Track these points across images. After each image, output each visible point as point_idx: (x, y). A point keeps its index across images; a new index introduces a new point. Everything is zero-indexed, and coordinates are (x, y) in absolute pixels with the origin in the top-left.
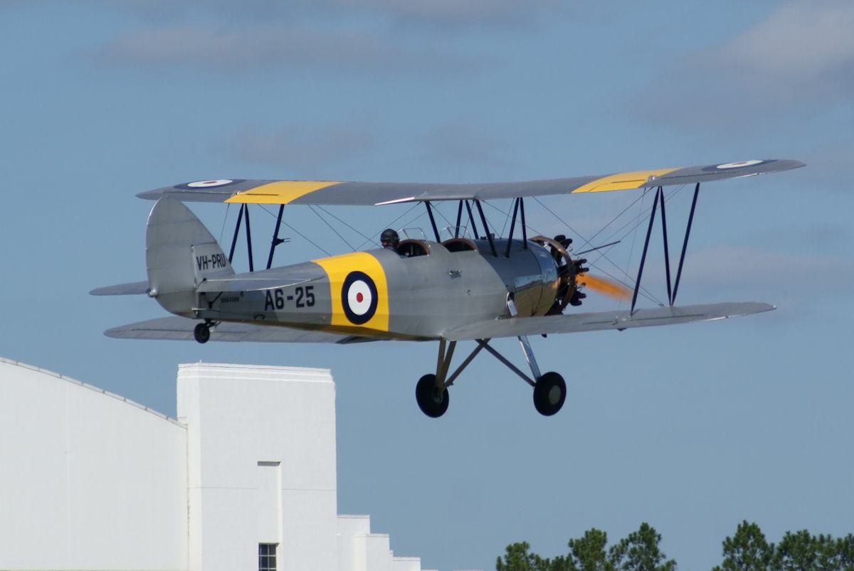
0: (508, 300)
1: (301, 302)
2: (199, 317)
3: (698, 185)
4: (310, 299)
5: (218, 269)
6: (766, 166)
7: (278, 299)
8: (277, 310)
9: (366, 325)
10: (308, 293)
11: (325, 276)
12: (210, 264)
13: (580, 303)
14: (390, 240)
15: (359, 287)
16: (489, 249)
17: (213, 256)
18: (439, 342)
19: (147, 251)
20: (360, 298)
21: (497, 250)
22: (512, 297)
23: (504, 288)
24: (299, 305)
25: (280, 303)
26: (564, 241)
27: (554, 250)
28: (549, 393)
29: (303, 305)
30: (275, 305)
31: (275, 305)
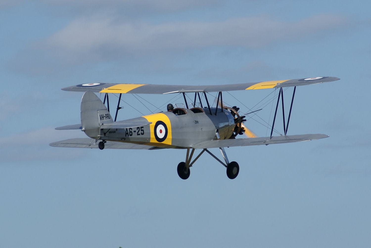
0: (216, 132)
1: (139, 133)
2: (100, 139)
3: (295, 87)
4: (142, 132)
5: (108, 120)
6: (324, 79)
7: (130, 132)
8: (130, 136)
9: (163, 142)
10: (141, 130)
12: (105, 118)
13: (242, 134)
14: (170, 108)
15: (161, 127)
16: (209, 112)
17: (106, 115)
18: (187, 149)
19: (81, 112)
20: (161, 131)
21: (212, 112)
22: (217, 131)
23: (215, 128)
24: (138, 134)
25: (131, 134)
26: (236, 109)
27: (232, 112)
28: (232, 170)
29: (139, 134)
30: (129, 134)
31: (129, 134)
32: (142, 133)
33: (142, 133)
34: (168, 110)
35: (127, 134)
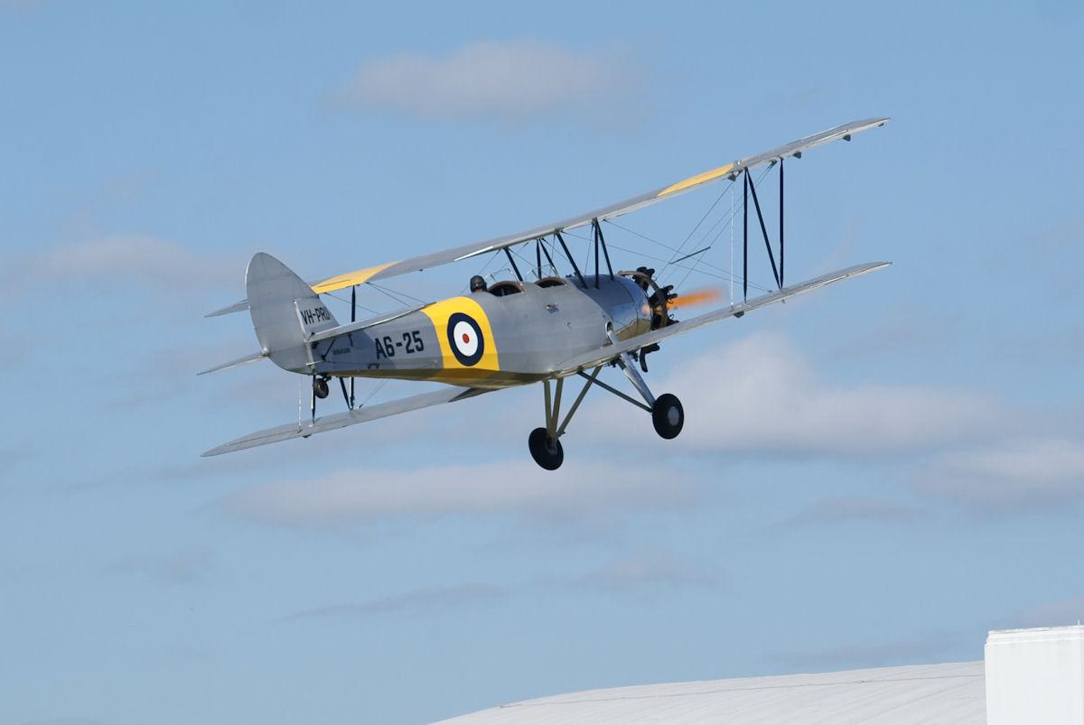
1: (410, 348)
4: (419, 344)
5: (323, 322)
7: (388, 346)
8: (391, 358)
9: (477, 366)
10: (414, 339)
11: (429, 320)
12: (315, 318)
15: (462, 328)
17: (316, 310)
20: (466, 339)
21: (588, 285)
25: (390, 350)
28: (667, 415)
29: (413, 351)
32: (420, 346)
33: (420, 346)
34: (474, 289)
35: (380, 351)
